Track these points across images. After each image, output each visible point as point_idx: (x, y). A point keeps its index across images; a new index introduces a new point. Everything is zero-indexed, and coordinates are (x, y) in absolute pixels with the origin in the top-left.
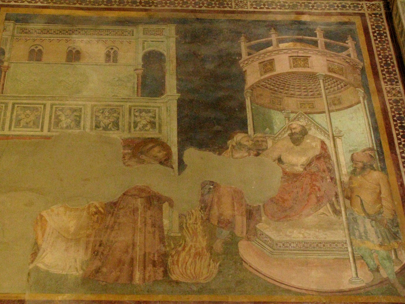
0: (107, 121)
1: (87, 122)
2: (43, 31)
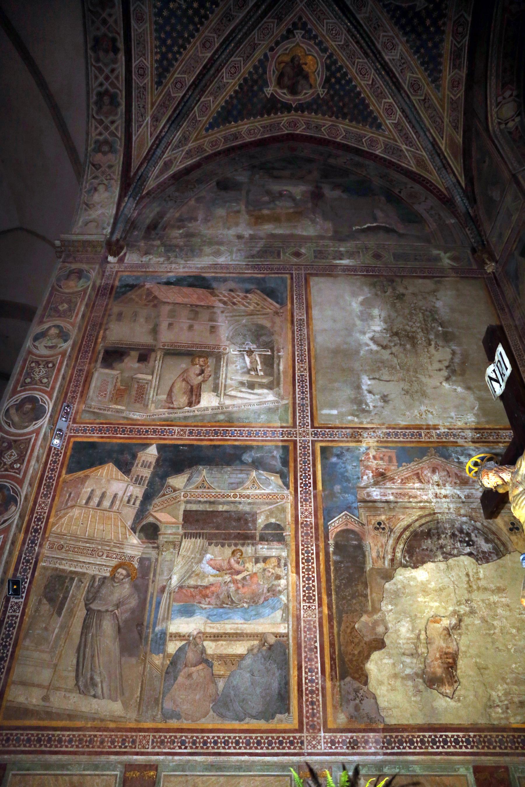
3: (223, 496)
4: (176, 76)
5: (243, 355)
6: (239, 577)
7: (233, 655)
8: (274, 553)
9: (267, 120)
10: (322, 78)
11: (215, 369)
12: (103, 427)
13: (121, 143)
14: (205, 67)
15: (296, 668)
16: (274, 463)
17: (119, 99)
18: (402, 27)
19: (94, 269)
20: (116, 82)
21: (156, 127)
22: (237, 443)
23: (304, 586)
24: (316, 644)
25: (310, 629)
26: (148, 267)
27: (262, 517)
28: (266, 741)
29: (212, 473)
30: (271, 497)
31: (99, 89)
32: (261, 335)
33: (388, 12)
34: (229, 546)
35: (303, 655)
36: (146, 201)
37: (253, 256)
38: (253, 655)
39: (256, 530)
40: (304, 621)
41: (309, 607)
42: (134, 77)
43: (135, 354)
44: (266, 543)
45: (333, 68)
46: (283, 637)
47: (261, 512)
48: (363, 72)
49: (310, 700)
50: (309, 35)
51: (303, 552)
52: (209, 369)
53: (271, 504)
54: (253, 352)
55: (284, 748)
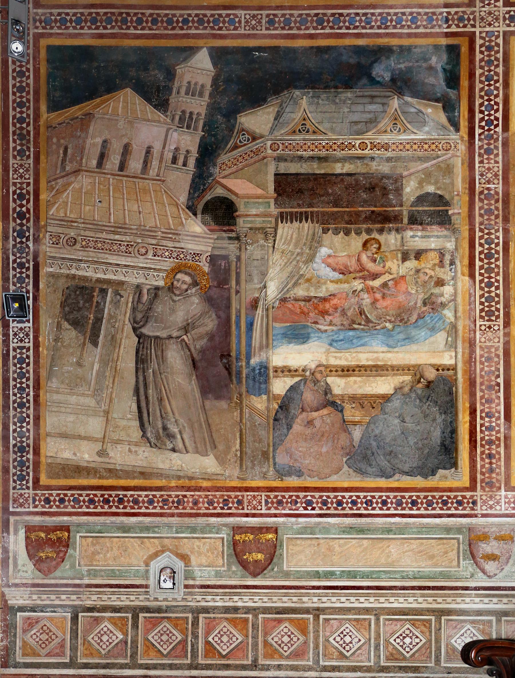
3: (342, 147)
6: (377, 283)
7: (372, 396)
8: (433, 244)
12: (98, 14)
15: (468, 412)
16: (431, 80)
22: (361, 42)
23: (482, 296)
24: (498, 380)
25: (489, 359)
27: (412, 183)
28: (425, 501)
29: (318, 104)
30: (426, 146)
34: (358, 233)
35: (479, 394)
38: (403, 395)
39: (401, 206)
40: (481, 347)
41: (490, 327)
44: (420, 227)
46: (448, 370)
47: (410, 175)
49: (487, 452)
51: (483, 241)
53: (427, 159)
55: (449, 509)
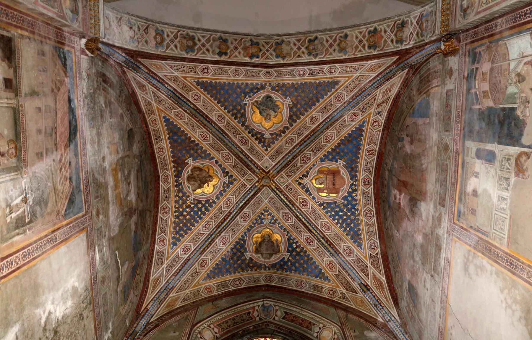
0: (505, 184)
1: (506, 194)
2: (464, 206)
4: (202, 95)
5: (22, 194)
9: (169, 160)
10: (200, 198)
11: (7, 168)
13: (163, 52)
14: (207, 116)
17: (190, 53)
18: (235, 247)
19: (79, 27)
20: (201, 51)
21: (170, 79)
26: (80, 79)
31: (197, 38)
32: (40, 206)
33: (242, 236)
36: (119, 69)
37: (93, 175)
42: (202, 65)
43: (10, 74)
45: (207, 205)
48: (207, 226)
50: (226, 186)
52: (6, 161)
54: (26, 203)
